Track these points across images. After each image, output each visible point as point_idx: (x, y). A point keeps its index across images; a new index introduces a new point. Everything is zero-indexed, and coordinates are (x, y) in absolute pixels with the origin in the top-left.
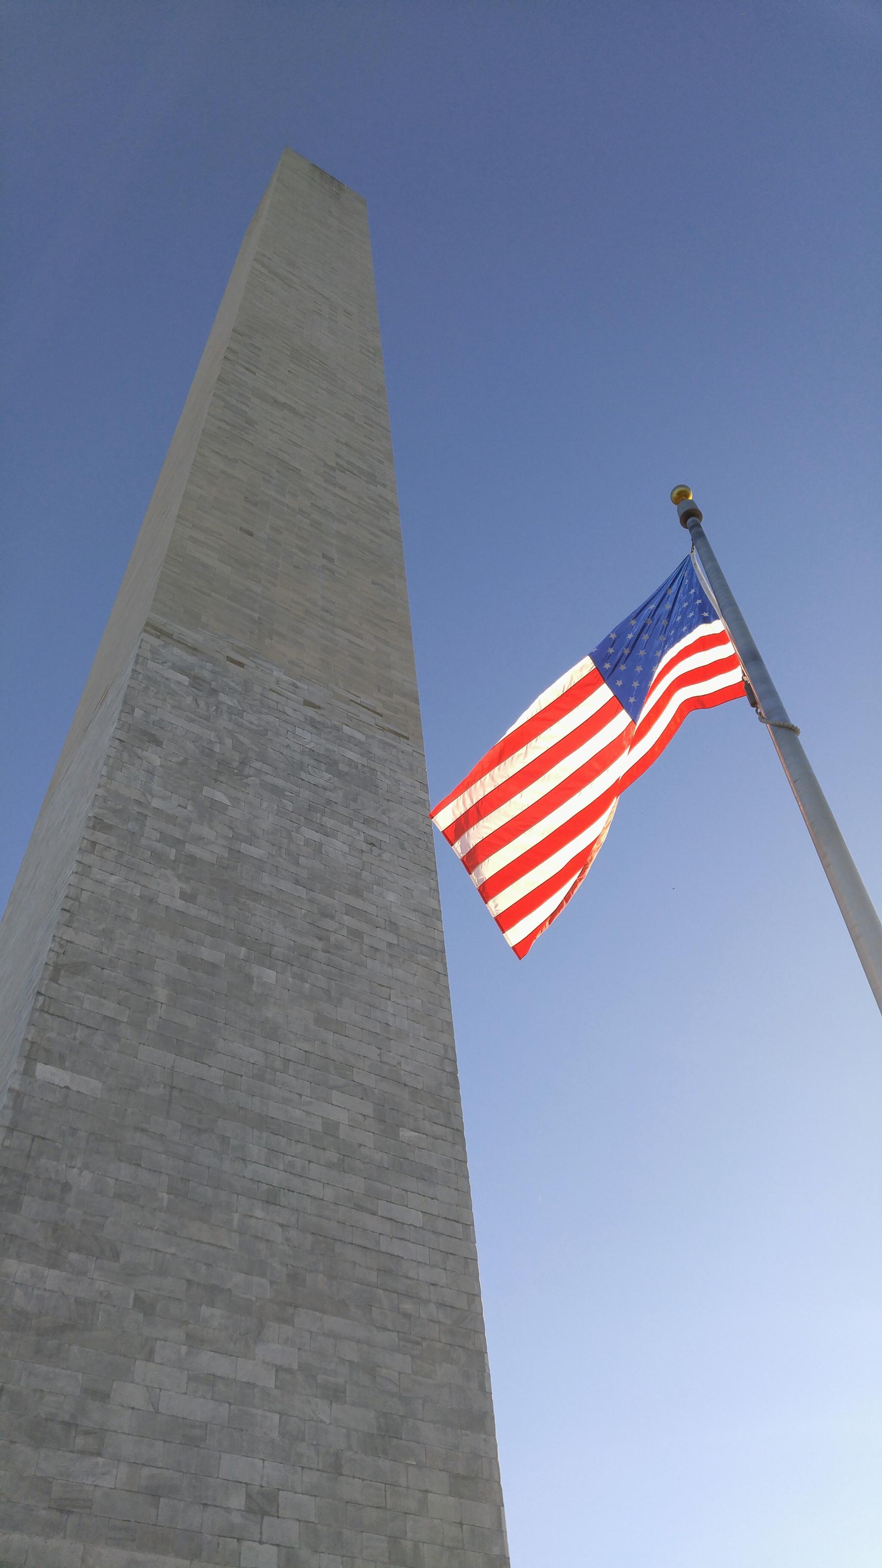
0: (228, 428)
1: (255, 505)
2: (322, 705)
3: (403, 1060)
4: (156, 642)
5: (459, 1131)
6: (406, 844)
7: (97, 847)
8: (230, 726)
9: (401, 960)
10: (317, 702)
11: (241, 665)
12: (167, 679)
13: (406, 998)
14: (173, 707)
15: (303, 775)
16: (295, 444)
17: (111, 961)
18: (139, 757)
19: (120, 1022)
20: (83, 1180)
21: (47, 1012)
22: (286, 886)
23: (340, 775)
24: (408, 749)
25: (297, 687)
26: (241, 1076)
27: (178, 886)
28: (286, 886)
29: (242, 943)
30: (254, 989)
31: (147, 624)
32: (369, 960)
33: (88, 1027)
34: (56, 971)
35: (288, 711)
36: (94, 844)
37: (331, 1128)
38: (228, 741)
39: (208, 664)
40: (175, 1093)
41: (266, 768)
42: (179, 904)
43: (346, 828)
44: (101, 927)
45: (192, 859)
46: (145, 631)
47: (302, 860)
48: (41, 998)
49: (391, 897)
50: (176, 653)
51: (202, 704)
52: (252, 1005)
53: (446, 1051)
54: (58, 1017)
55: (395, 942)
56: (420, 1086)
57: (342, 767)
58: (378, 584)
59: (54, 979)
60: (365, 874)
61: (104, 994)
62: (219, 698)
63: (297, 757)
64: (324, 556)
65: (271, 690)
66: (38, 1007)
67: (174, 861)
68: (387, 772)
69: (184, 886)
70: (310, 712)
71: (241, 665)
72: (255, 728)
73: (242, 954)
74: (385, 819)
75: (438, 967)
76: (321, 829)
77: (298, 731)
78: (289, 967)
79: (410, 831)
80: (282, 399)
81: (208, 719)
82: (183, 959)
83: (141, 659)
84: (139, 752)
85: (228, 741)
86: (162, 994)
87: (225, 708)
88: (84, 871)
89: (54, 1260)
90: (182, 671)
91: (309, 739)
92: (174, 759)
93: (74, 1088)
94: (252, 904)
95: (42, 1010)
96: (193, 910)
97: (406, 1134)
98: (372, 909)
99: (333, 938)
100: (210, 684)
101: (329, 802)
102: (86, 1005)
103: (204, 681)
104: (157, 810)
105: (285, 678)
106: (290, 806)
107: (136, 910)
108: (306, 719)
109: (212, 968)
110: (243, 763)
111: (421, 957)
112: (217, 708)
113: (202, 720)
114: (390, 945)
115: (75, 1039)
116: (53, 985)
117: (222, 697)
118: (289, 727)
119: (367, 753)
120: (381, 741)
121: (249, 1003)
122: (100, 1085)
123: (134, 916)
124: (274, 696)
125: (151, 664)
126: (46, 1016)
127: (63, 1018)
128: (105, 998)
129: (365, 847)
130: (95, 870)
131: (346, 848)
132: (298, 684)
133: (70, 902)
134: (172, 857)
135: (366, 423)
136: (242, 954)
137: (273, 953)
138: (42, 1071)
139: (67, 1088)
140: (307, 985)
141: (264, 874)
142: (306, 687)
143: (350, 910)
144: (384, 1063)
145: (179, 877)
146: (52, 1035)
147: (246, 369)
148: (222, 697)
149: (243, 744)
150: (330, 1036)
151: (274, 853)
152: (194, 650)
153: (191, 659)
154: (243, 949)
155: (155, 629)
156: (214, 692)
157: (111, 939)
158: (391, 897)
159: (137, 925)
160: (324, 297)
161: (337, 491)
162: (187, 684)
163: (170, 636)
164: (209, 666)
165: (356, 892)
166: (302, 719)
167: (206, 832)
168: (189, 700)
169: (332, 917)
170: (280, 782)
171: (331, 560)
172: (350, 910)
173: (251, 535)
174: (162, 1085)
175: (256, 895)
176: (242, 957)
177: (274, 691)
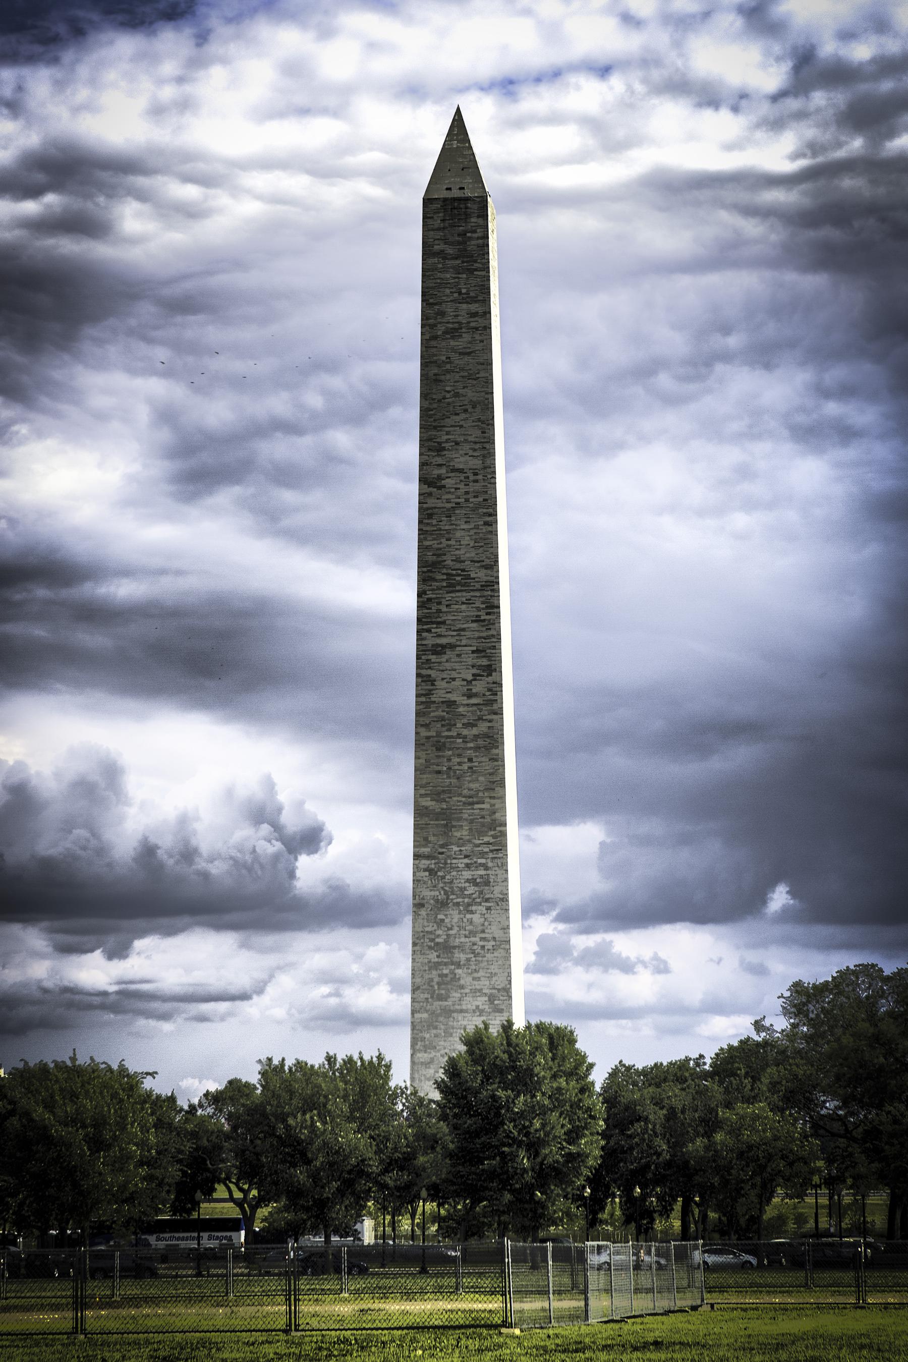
0: (423, 699)
5: (511, 997)
11: (442, 853)
15: (466, 892)
20: (427, 1036)
22: (463, 940)
23: (476, 884)
24: (500, 855)
27: (435, 954)
28: (463, 940)
35: (460, 865)
37: (477, 1007)
41: (454, 897)
42: (436, 960)
43: (480, 907)
45: (438, 944)
57: (478, 880)
63: (463, 885)
68: (493, 873)
70: (466, 861)
71: (442, 853)
74: (492, 896)
75: (507, 947)
76: (472, 912)
77: (463, 873)
79: (501, 896)
81: (435, 886)
86: (436, 987)
89: (425, 1052)
90: (425, 870)
91: (467, 874)
96: (440, 960)
97: (496, 1002)
101: (474, 899)
104: (427, 932)
106: (461, 908)
109: (446, 975)
110: (448, 899)
119: (487, 868)
120: (493, 858)
124: (454, 861)
125: (418, 874)
129: (485, 912)
135: (487, 614)
138: (417, 1015)
143: (482, 939)
148: (440, 874)
150: (476, 983)
152: (428, 857)
153: (427, 862)
158: (493, 928)
164: (433, 861)
165: (483, 931)
167: (439, 932)
170: (458, 900)
172: (482, 939)
175: (454, 947)
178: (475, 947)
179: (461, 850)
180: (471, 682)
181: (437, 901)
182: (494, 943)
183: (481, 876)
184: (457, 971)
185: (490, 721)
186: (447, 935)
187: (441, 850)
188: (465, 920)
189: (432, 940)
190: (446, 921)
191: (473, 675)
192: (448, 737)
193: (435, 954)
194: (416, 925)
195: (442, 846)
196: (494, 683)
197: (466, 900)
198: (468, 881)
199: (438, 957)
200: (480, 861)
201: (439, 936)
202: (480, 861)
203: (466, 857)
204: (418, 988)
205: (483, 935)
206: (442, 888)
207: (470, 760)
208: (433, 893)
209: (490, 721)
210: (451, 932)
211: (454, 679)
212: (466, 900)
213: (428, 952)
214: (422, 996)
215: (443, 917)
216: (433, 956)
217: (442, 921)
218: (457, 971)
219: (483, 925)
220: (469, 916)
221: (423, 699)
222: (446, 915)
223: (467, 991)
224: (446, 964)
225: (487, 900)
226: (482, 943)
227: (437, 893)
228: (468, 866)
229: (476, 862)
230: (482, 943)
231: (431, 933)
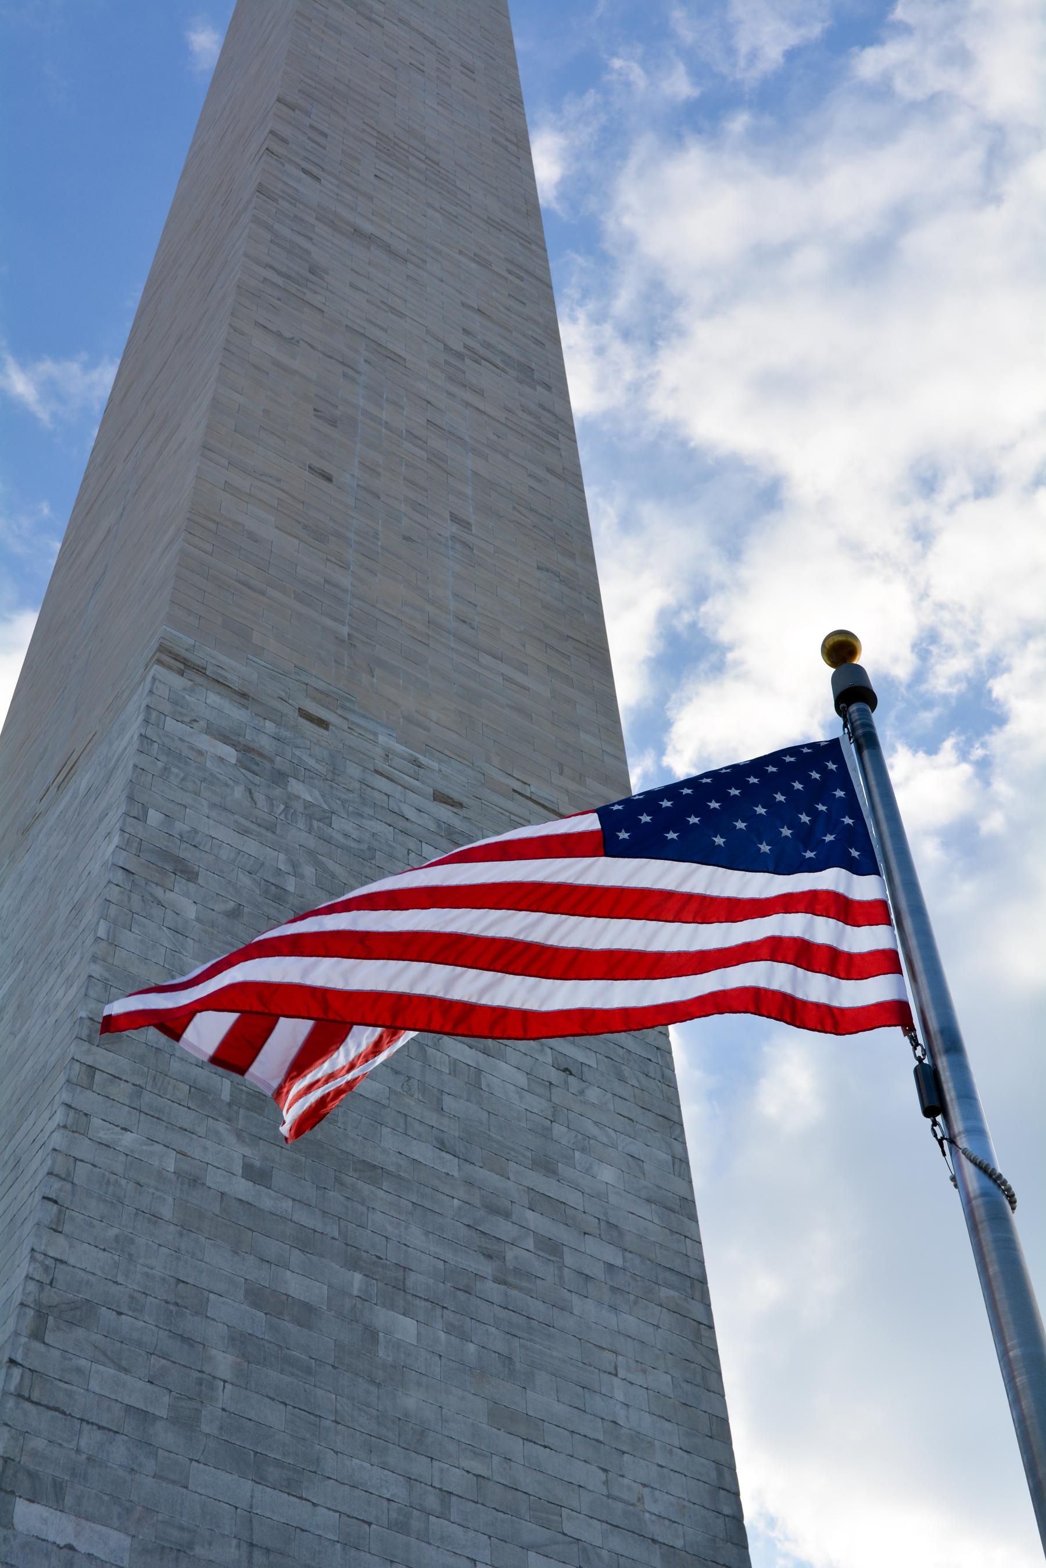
0: (279, 280)
1: (333, 423)
2: (465, 800)
3: (646, 1490)
4: (178, 682)
6: (627, 1072)
7: (98, 1076)
8: (312, 843)
9: (632, 1297)
10: (456, 796)
11: (322, 724)
12: (200, 753)
13: (644, 1371)
14: (213, 805)
16: (393, 310)
17: (132, 1297)
18: (159, 903)
19: (156, 1418)
21: (29, 1399)
22: (424, 1152)
25: (420, 766)
26: (370, 1524)
27: (237, 1152)
28: (424, 1152)
29: (353, 1263)
30: (381, 1354)
31: (162, 649)
32: (575, 1298)
33: (100, 1427)
34: (42, 1318)
36: (92, 1069)
38: (309, 871)
39: (268, 723)
40: (258, 1556)
42: (242, 1188)
44: (113, 1232)
46: (159, 662)
47: (448, 1102)
48: (16, 1372)
49: (607, 1175)
50: (212, 703)
51: (260, 798)
52: (379, 1385)
53: (720, 1474)
54: (48, 1408)
55: (619, 1262)
56: (679, 1543)
58: (548, 570)
59: (37, 1335)
60: (558, 1130)
61: (124, 1363)
62: (289, 789)
64: (454, 518)
65: (377, 772)
66: (12, 1388)
67: (230, 1104)
69: (248, 1152)
70: (444, 812)
71: (322, 724)
72: (353, 844)
73: (356, 1286)
78: (438, 1311)
80: (368, 228)
81: (271, 828)
83: (154, 714)
84: (159, 892)
85: (309, 871)
86: (223, 1362)
87: (299, 807)
88: (77, 1122)
90: (225, 738)
92: (220, 907)
93: (82, 1548)
94: (366, 1188)
95: (19, 1396)
96: (267, 1201)
98: (573, 1198)
99: (511, 1254)
100: (272, 761)
102: (94, 1385)
103: (261, 755)
105: (400, 748)
107: (170, 1200)
108: (439, 826)
109: (306, 1314)
111: (664, 1293)
112: (287, 807)
113: (263, 831)
114: (610, 1267)
115: (78, 1451)
116: (37, 1345)
117: (296, 787)
118: (412, 844)
121: (372, 1382)
122: (127, 1541)
123: (167, 1211)
125: (170, 724)
126: (27, 1405)
127: (55, 1409)
128: (126, 1371)
129: (555, 1076)
130: (96, 1122)
131: (522, 1080)
132: (422, 759)
133: (57, 1184)
134: (226, 1096)
135: (510, 272)
136: (356, 1286)
137: (410, 1284)
139: (70, 1547)
140: (472, 1348)
141: (385, 1130)
142: (435, 765)
143: (538, 1201)
144: (615, 1498)
145: (239, 1134)
146: (39, 1443)
147: (304, 171)
148: (296, 787)
149: (333, 876)
150: (516, 1447)
151: (399, 1089)
152: (243, 697)
153: (236, 714)
154: (358, 1277)
155: (176, 657)
156: (279, 777)
157: (130, 1255)
159: (172, 1228)
160: (426, 38)
161: (469, 396)
162: (234, 761)
163: (200, 670)
164: (270, 726)
165: (546, 1166)
166: (433, 827)
168: (239, 792)
169: (507, 1215)
171: (466, 525)
172: (538, 1201)
173: (329, 479)
174: (234, 1542)
175: (372, 1172)
176: (355, 1293)
177: (382, 774)
178: (504, 1229)
179: (415, 762)
180: (460, 356)
184: (382, 1317)
191: (466, 347)
194: (128, 939)
195: (323, 697)
204: (78, 1313)
206: (312, 854)
208: (251, 846)
213: (185, 1118)
214: (101, 1377)
218: (382, 1317)
219: (546, 1134)
223: (456, 1480)
224: (307, 1242)
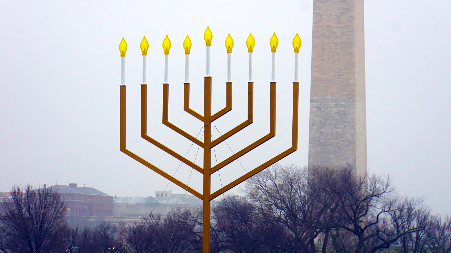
0: (316, 25)
11: (324, 99)
15: (335, 118)
22: (333, 141)
24: (352, 101)
27: (320, 148)
28: (333, 141)
43: (341, 126)
45: (321, 143)
50: (315, 104)
70: (335, 103)
71: (324, 99)
76: (337, 128)
82: (322, 158)
124: (330, 103)
125: (312, 109)
152: (317, 102)
153: (317, 104)
158: (348, 135)
165: (342, 137)
167: (322, 137)
170: (331, 122)
172: (342, 141)
181: (321, 123)
182: (347, 143)
183: (342, 111)
185: (348, 35)
186: (326, 139)
187: (324, 98)
188: (334, 132)
189: (318, 141)
190: (325, 132)
191: (341, 13)
192: (328, 43)
193: (320, 148)
196: (350, 17)
197: (335, 122)
198: (336, 113)
199: (321, 149)
200: (342, 103)
201: (322, 139)
202: (342, 103)
203: (335, 101)
205: (343, 139)
207: (338, 54)
208: (319, 119)
209: (348, 35)
210: (328, 137)
211: (331, 15)
212: (335, 122)
215: (323, 130)
216: (319, 149)
217: (323, 132)
219: (343, 134)
220: (336, 130)
221: (316, 25)
222: (325, 129)
225: (344, 122)
226: (341, 143)
227: (321, 119)
228: (336, 106)
229: (340, 104)
230: (341, 143)
231: (318, 137)
